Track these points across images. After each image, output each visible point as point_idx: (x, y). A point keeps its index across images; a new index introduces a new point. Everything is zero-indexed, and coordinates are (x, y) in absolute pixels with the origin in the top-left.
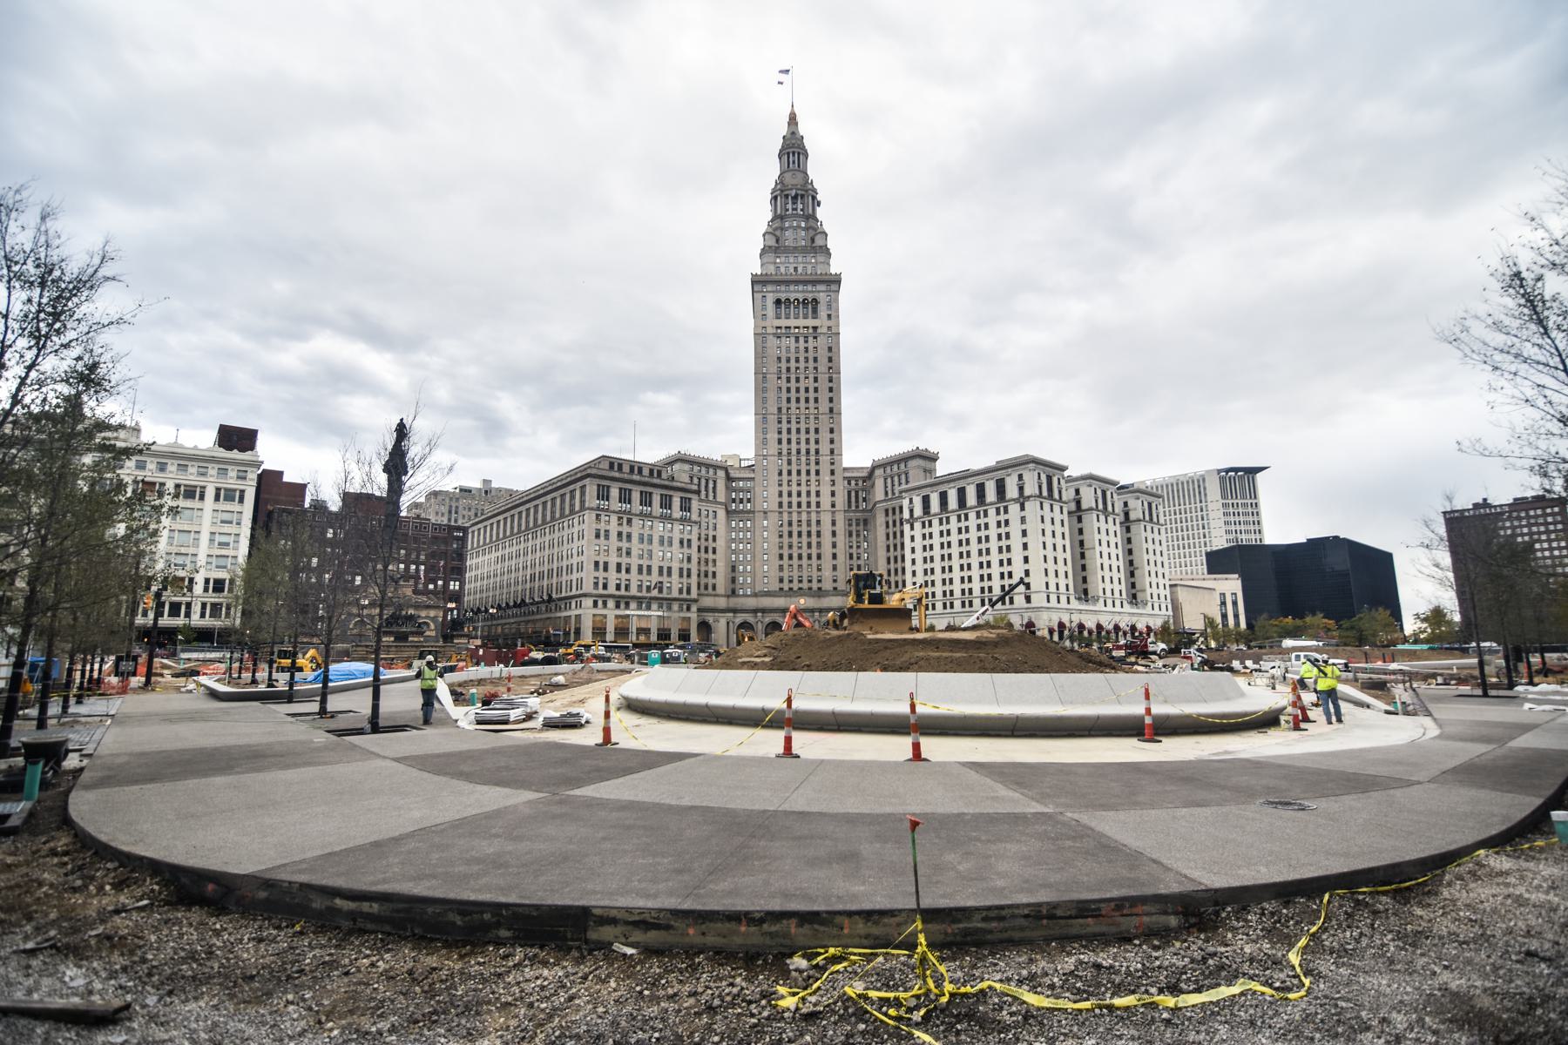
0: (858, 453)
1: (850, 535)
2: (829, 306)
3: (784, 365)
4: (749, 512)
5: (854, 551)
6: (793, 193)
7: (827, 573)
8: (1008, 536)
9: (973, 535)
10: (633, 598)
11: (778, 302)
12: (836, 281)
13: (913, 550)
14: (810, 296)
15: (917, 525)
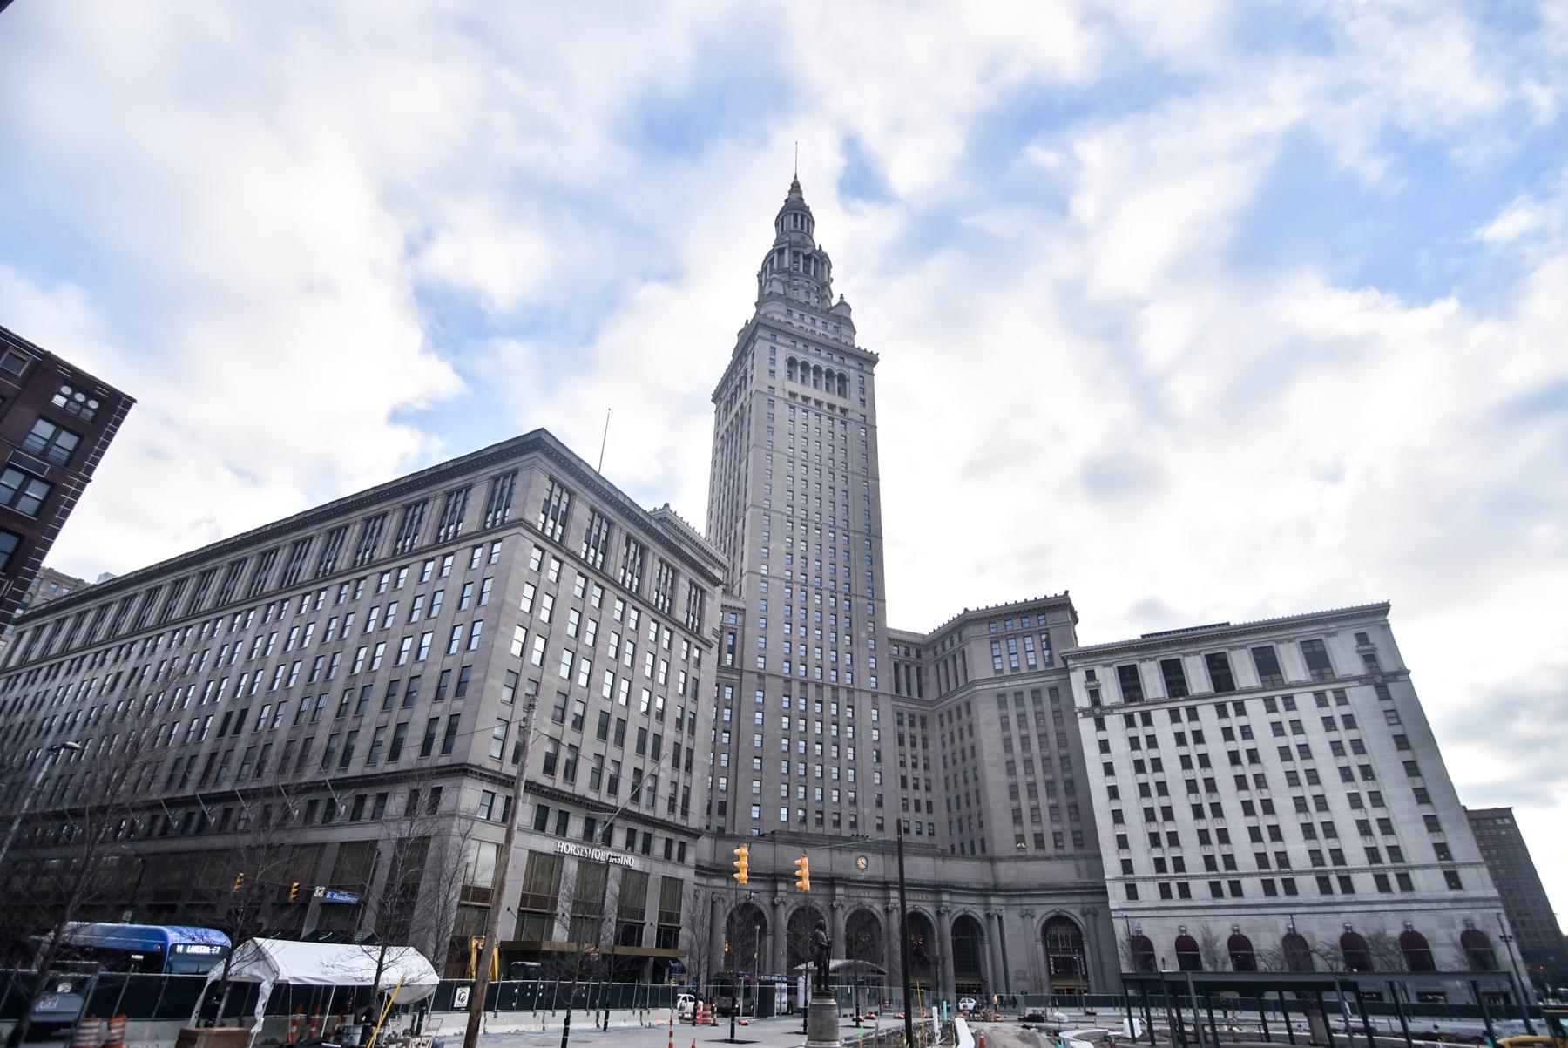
0: (916, 604)
1: (901, 742)
2: (863, 390)
3: (800, 444)
4: (731, 669)
5: (909, 772)
6: (807, 252)
7: (867, 811)
8: (1358, 747)
9: (1266, 743)
10: (580, 802)
11: (792, 362)
12: (869, 360)
13: (1109, 769)
14: (837, 370)
15: (1114, 722)
